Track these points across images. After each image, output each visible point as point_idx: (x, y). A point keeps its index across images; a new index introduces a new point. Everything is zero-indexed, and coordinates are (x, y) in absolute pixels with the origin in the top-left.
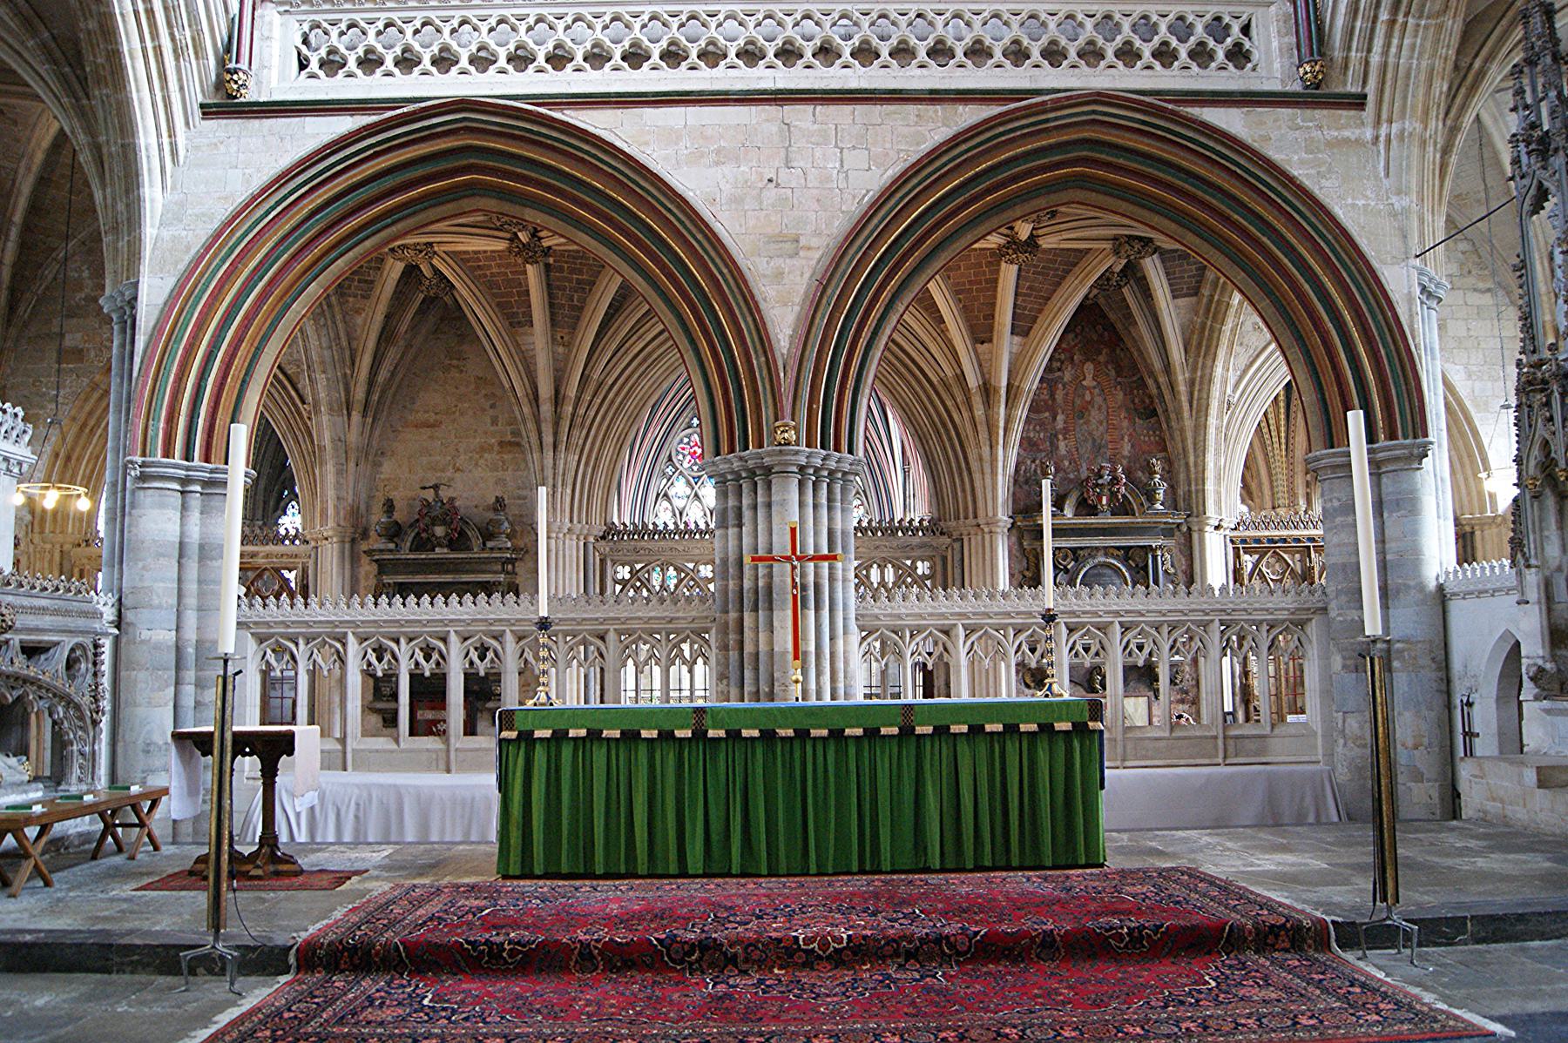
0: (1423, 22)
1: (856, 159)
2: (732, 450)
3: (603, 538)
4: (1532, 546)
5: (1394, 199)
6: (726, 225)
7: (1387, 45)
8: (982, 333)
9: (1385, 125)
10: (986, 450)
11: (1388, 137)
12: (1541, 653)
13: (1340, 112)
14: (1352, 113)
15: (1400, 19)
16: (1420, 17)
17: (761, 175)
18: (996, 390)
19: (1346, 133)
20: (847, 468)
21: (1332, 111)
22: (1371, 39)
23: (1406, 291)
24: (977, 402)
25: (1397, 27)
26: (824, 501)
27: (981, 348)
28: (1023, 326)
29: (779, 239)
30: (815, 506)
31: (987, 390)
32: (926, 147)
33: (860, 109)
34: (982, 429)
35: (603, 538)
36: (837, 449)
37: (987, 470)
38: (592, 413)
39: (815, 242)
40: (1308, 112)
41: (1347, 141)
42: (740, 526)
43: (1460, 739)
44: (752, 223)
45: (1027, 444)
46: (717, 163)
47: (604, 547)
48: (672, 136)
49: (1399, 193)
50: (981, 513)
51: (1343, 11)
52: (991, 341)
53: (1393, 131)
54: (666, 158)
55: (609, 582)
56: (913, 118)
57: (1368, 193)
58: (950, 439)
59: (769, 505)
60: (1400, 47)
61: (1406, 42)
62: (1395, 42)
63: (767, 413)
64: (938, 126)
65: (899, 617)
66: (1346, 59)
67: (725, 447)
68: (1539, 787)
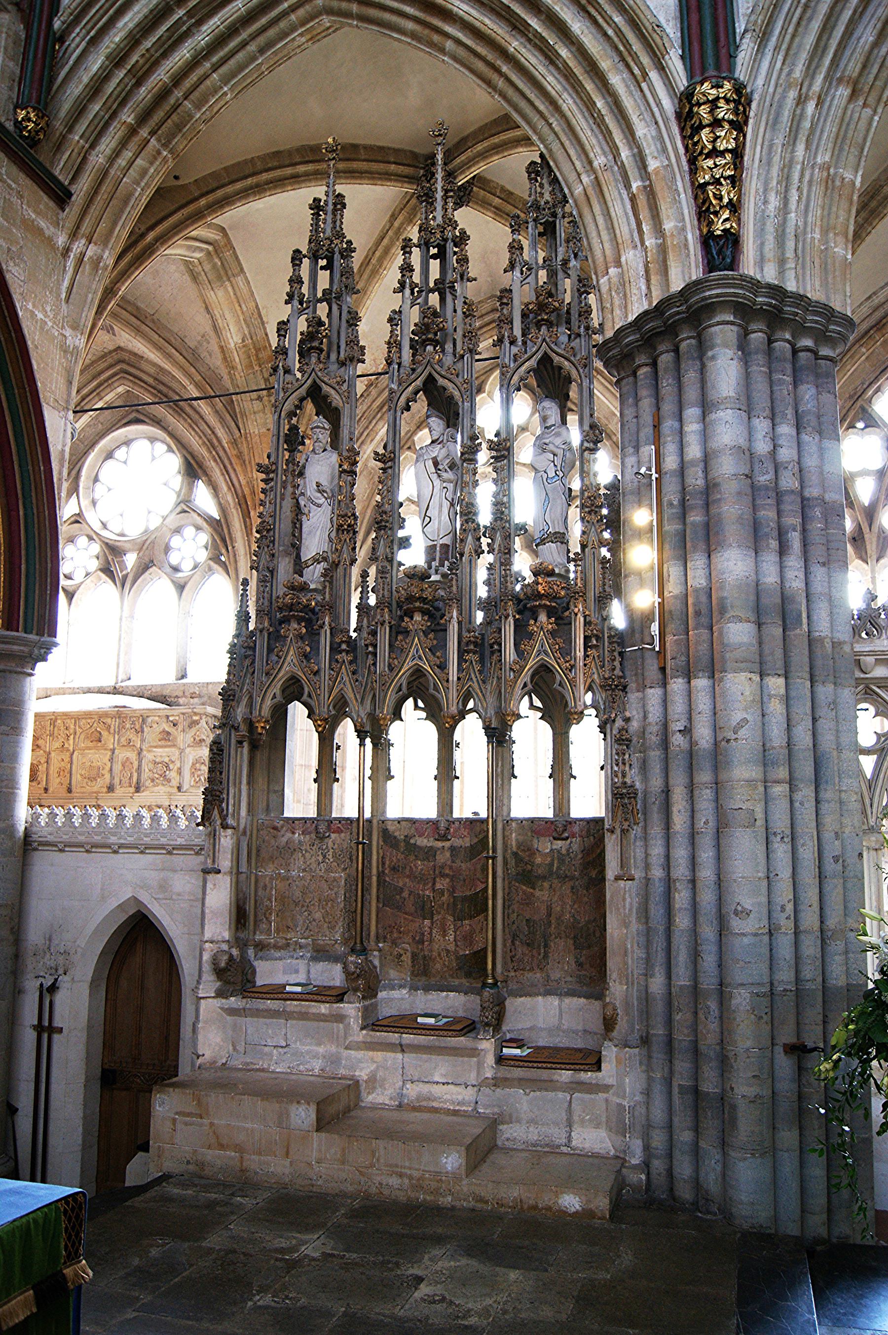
0: (165, 153)
4: (231, 801)
5: (68, 332)
7: (117, 153)
9: (83, 241)
11: (83, 254)
12: (226, 935)
13: (42, 193)
14: (52, 204)
15: (144, 133)
16: (165, 146)
19: (43, 224)
21: (36, 187)
22: (100, 135)
23: (60, 447)
25: (136, 140)
40: (14, 169)
41: (40, 231)
43: (28, 1038)
49: (75, 327)
51: (86, 80)
53: (89, 253)
57: (48, 309)
60: (131, 163)
61: (139, 161)
62: (128, 154)
66: (63, 138)
68: (318, 1129)
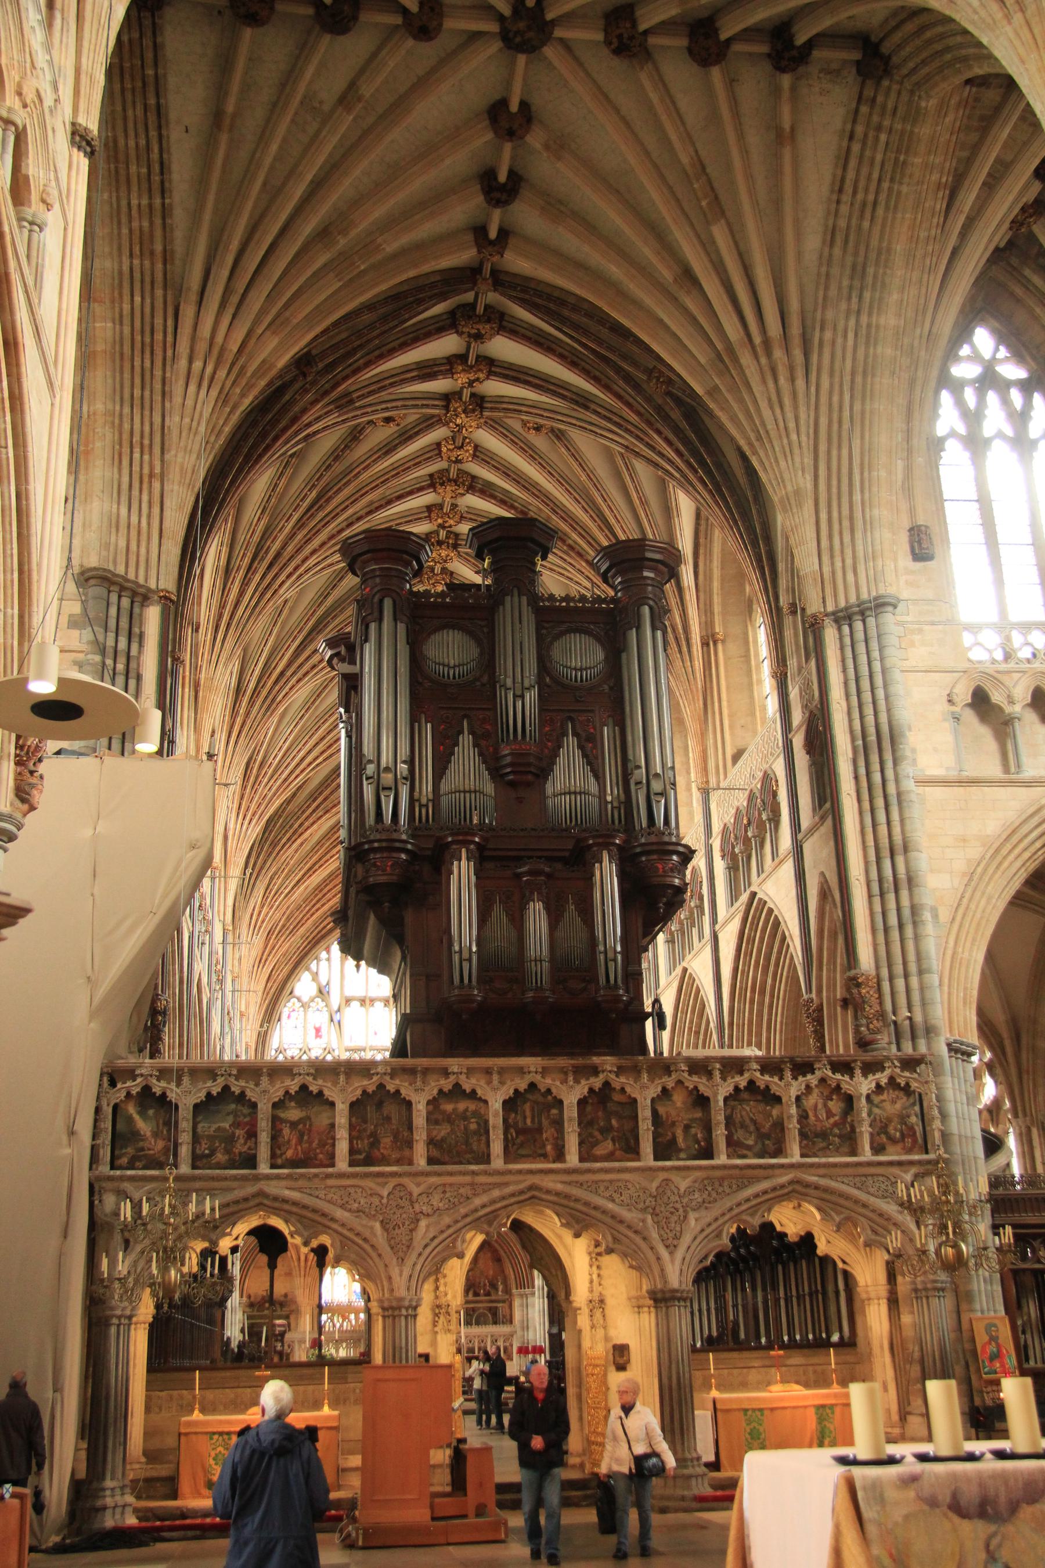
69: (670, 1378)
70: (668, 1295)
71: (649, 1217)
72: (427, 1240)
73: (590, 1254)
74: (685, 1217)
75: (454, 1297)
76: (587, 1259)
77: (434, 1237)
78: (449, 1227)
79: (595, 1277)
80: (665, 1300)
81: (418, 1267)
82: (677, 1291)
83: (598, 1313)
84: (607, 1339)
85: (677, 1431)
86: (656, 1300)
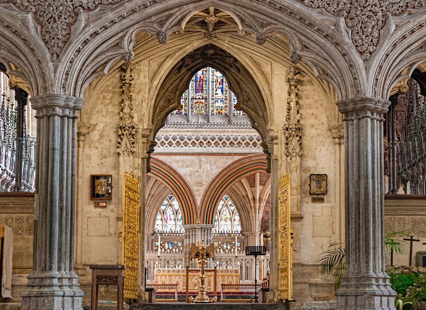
1: (214, 167)
2: (188, 224)
3: (152, 235)
6: (188, 180)
8: (253, 185)
10: (254, 214)
17: (195, 170)
18: (256, 199)
20: (211, 227)
24: (252, 202)
26: (206, 234)
27: (253, 188)
28: (263, 183)
29: (198, 183)
30: (204, 235)
31: (254, 199)
32: (227, 165)
33: (215, 156)
34: (253, 209)
35: (152, 235)
36: (209, 224)
37: (254, 219)
38: (151, 202)
39: (205, 184)
42: (189, 238)
44: (193, 180)
45: (266, 212)
46: (186, 167)
47: (152, 237)
48: (177, 162)
50: (252, 231)
52: (254, 187)
54: (177, 166)
55: (154, 247)
56: (225, 159)
58: (245, 210)
59: (195, 235)
63: (195, 217)
64: (230, 160)
65: (221, 257)
67: (187, 223)
69: (358, 195)
70: (359, 106)
71: (342, 20)
72: (87, 36)
73: (289, 81)
74: (385, 22)
75: (141, 120)
76: (286, 87)
77: (96, 34)
78: (113, 22)
79: (293, 104)
80: (356, 111)
81: (78, 66)
82: (370, 100)
83: (294, 142)
84: (302, 168)
85: (362, 250)
86: (346, 113)
